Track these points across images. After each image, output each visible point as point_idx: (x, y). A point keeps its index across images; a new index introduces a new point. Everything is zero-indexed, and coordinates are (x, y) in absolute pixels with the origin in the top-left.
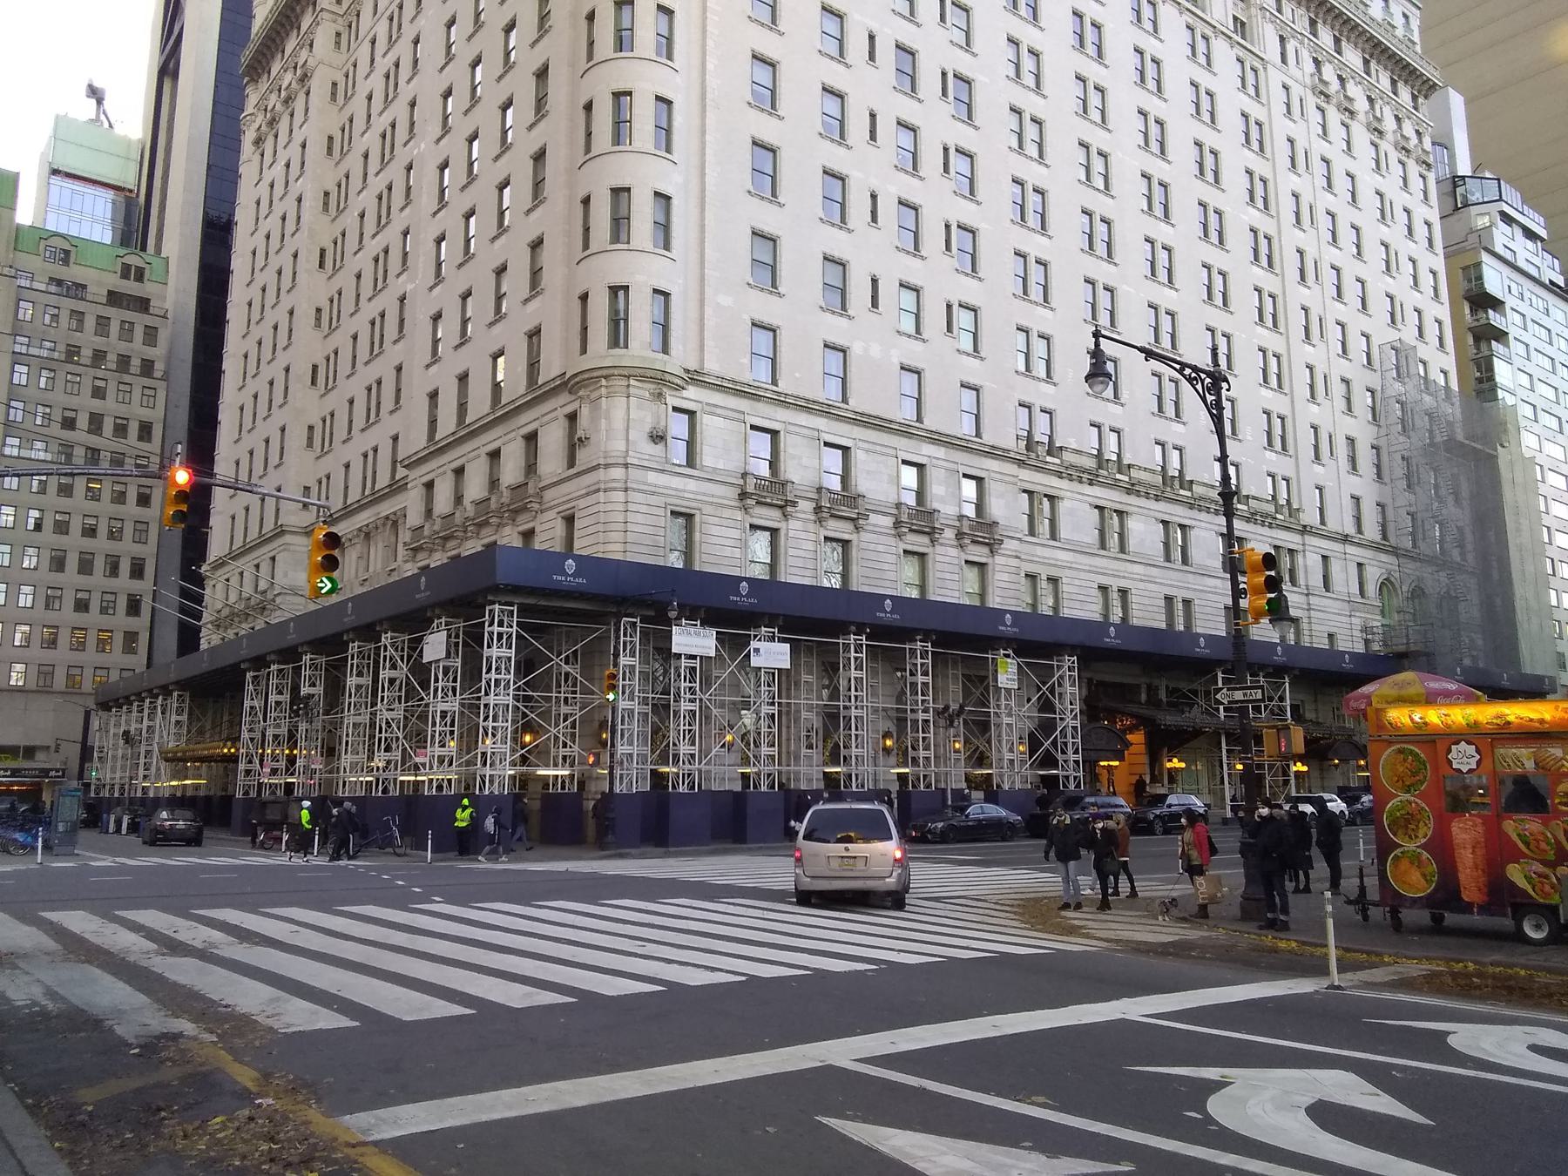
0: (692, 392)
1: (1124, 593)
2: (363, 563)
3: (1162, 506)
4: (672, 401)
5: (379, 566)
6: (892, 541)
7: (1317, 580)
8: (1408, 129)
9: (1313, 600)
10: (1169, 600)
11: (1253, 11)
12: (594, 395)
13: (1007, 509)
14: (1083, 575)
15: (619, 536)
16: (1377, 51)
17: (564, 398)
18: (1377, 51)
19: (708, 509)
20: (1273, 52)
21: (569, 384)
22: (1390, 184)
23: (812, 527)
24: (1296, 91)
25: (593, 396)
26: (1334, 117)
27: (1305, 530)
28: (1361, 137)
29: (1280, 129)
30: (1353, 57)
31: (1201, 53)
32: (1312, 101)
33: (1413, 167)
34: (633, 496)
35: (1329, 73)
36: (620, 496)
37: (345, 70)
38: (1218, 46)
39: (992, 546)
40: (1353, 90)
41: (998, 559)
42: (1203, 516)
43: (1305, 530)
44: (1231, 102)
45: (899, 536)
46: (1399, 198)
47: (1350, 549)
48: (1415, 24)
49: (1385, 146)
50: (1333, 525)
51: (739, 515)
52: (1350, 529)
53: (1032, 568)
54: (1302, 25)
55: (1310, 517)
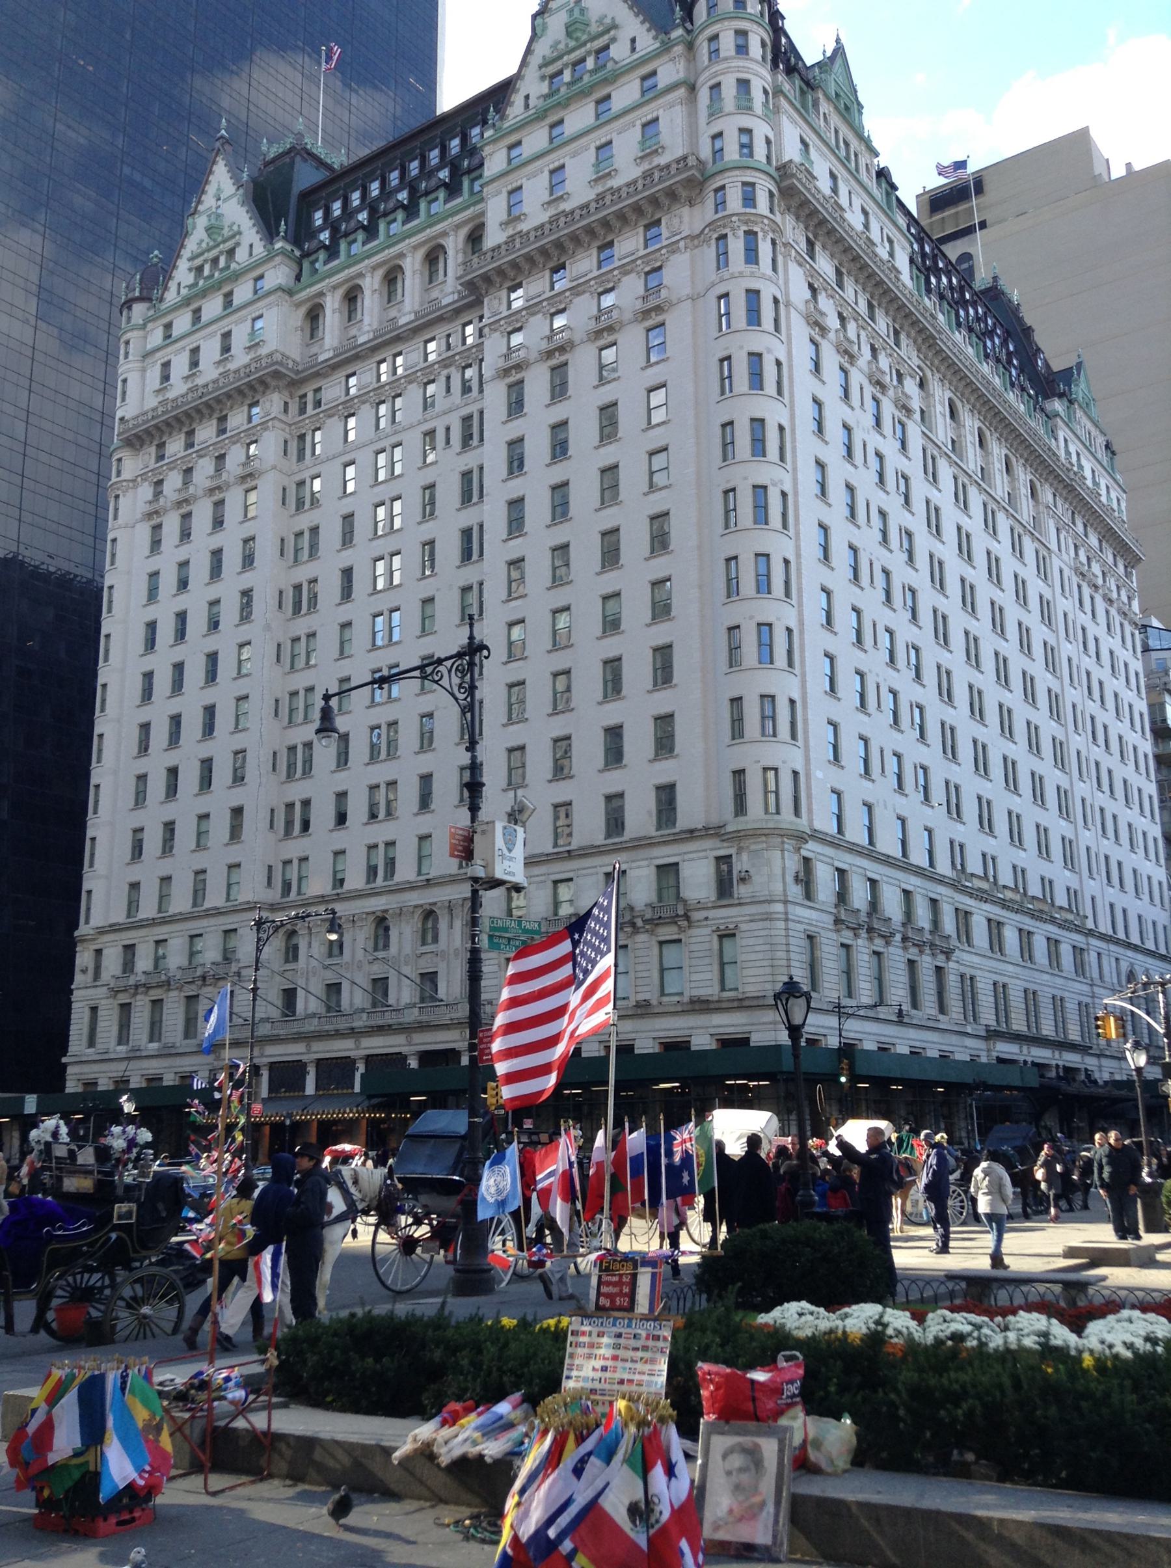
0: (811, 845)
1: (1004, 986)
2: (371, 944)
3: (1018, 917)
4: (804, 853)
5: (407, 950)
6: (900, 952)
7: (1096, 975)
8: (1124, 599)
9: (1096, 989)
10: (1025, 991)
11: (1041, 508)
12: (753, 847)
13: (949, 924)
14: (987, 974)
15: (782, 955)
16: (1109, 535)
17: (708, 844)
18: (1109, 535)
19: (822, 932)
20: (1053, 546)
21: (714, 831)
22: (1115, 643)
23: (866, 943)
24: (1067, 572)
25: (753, 847)
26: (1087, 591)
27: (1090, 933)
28: (1100, 605)
29: (1063, 605)
30: (1093, 540)
31: (1017, 549)
32: (1075, 580)
33: (1128, 629)
34: (791, 925)
35: (1083, 558)
36: (782, 924)
37: (298, 478)
38: (1027, 541)
39: (948, 954)
40: (1096, 568)
41: (952, 965)
42: (1038, 924)
43: (1090, 933)
44: (1035, 587)
45: (905, 948)
46: (1124, 655)
47: (1112, 947)
48: (1123, 505)
49: (1113, 612)
50: (1102, 929)
51: (834, 936)
52: (1110, 932)
53: (963, 970)
54: (1067, 519)
55: (1090, 924)
